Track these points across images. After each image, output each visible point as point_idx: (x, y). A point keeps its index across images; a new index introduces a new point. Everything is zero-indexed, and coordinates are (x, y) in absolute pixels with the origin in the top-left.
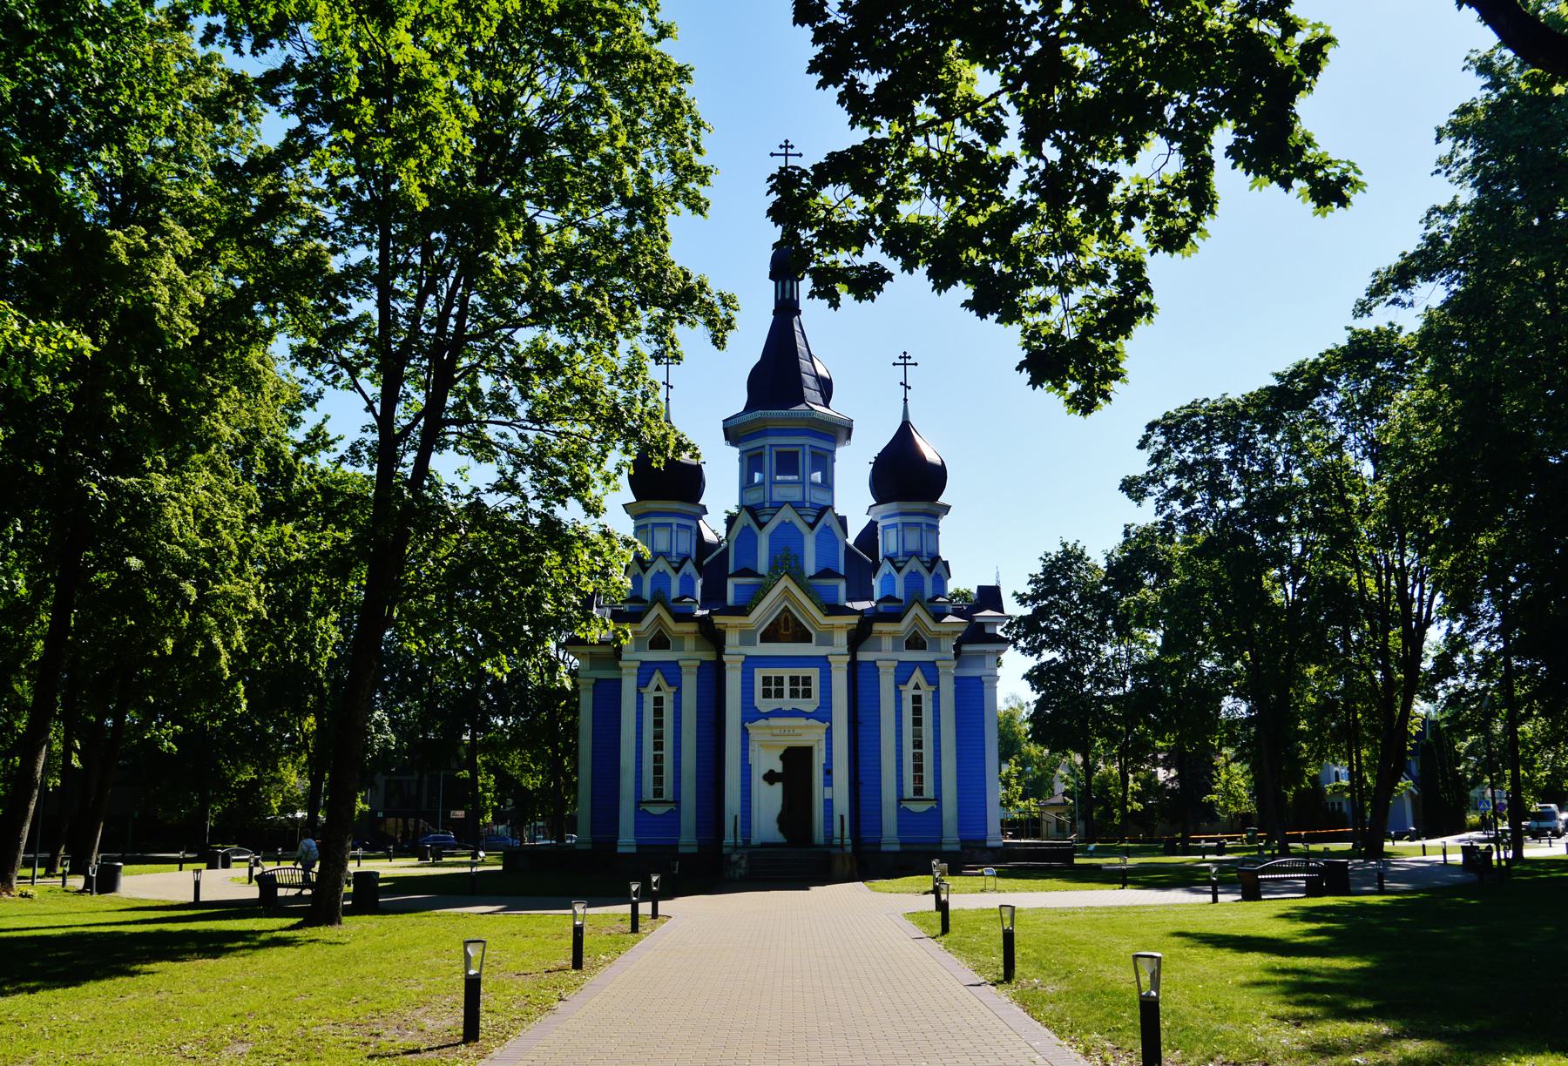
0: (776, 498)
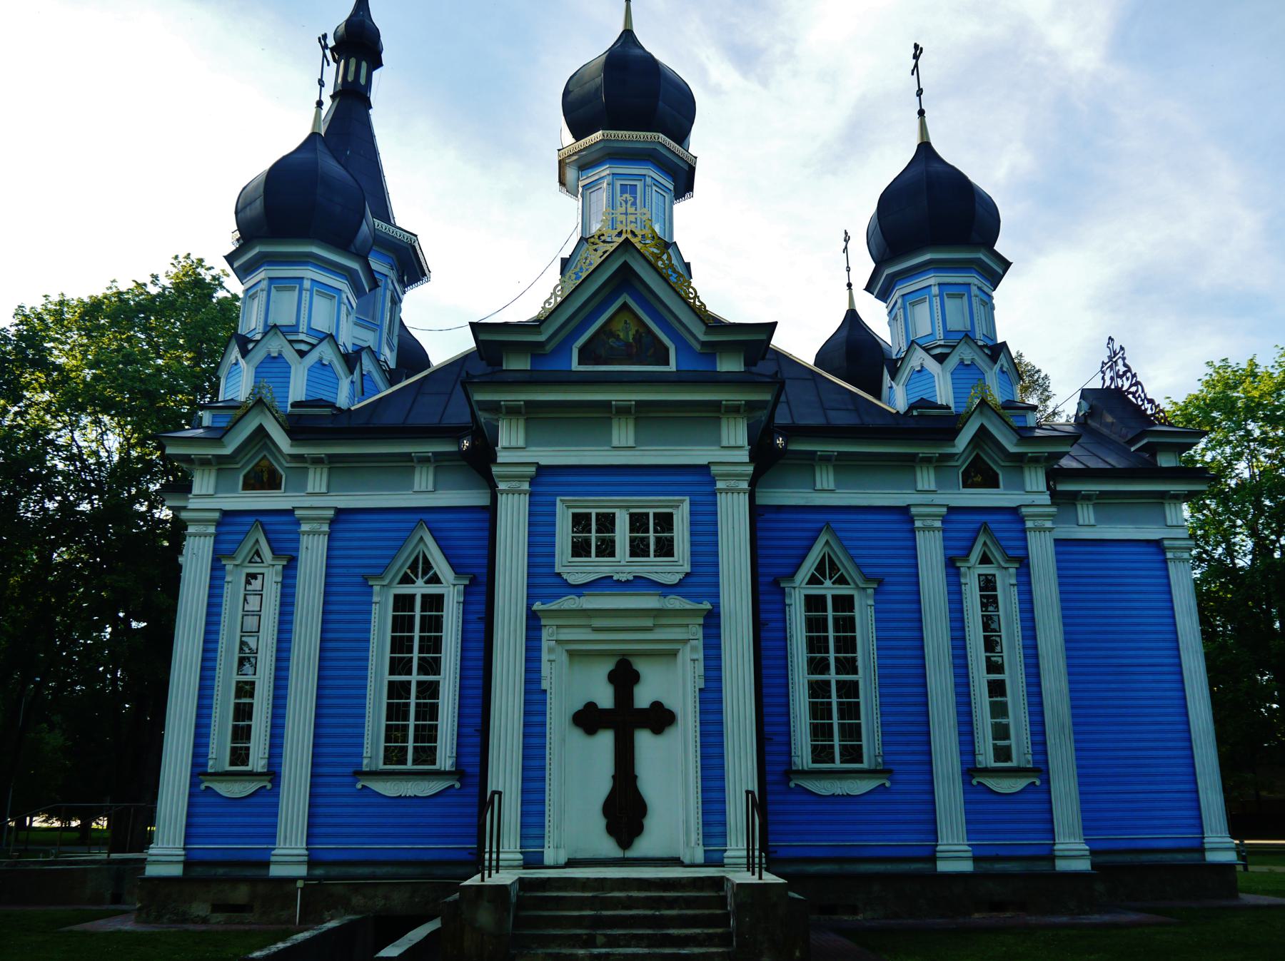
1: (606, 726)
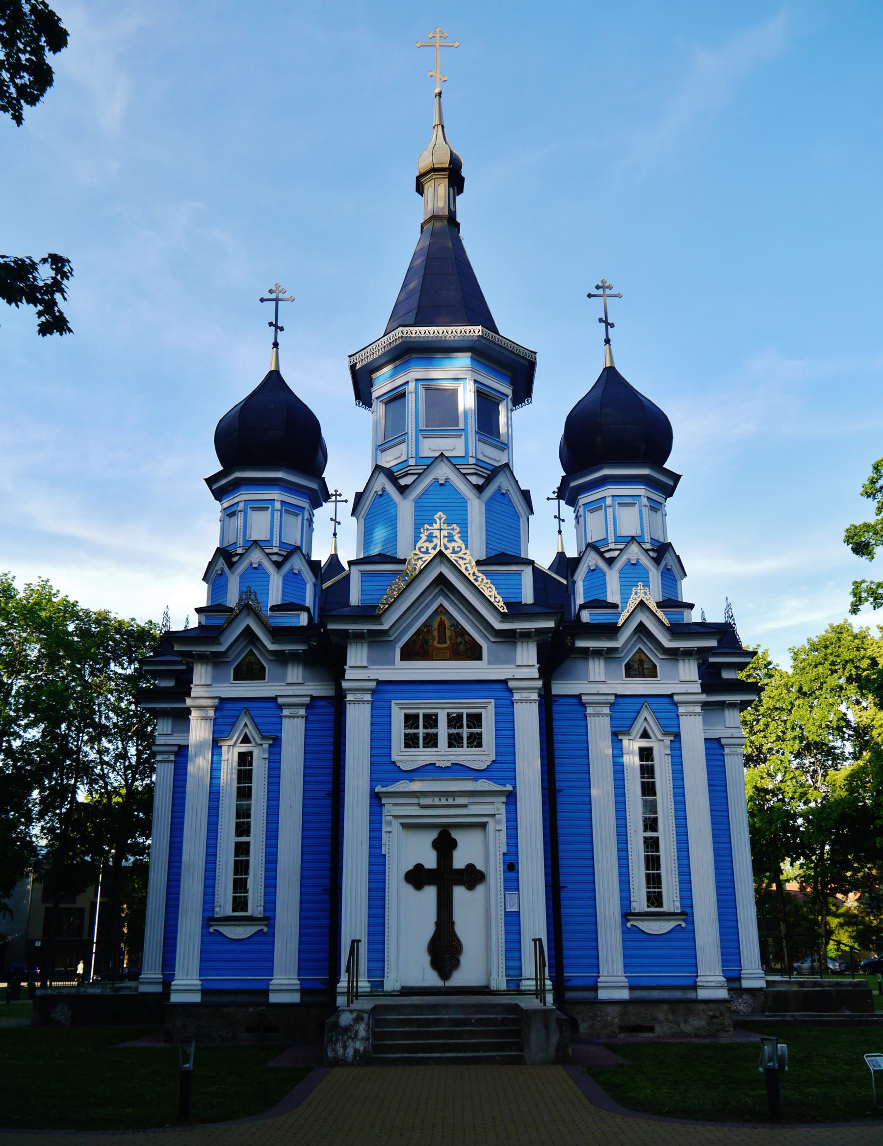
1: (430, 883)
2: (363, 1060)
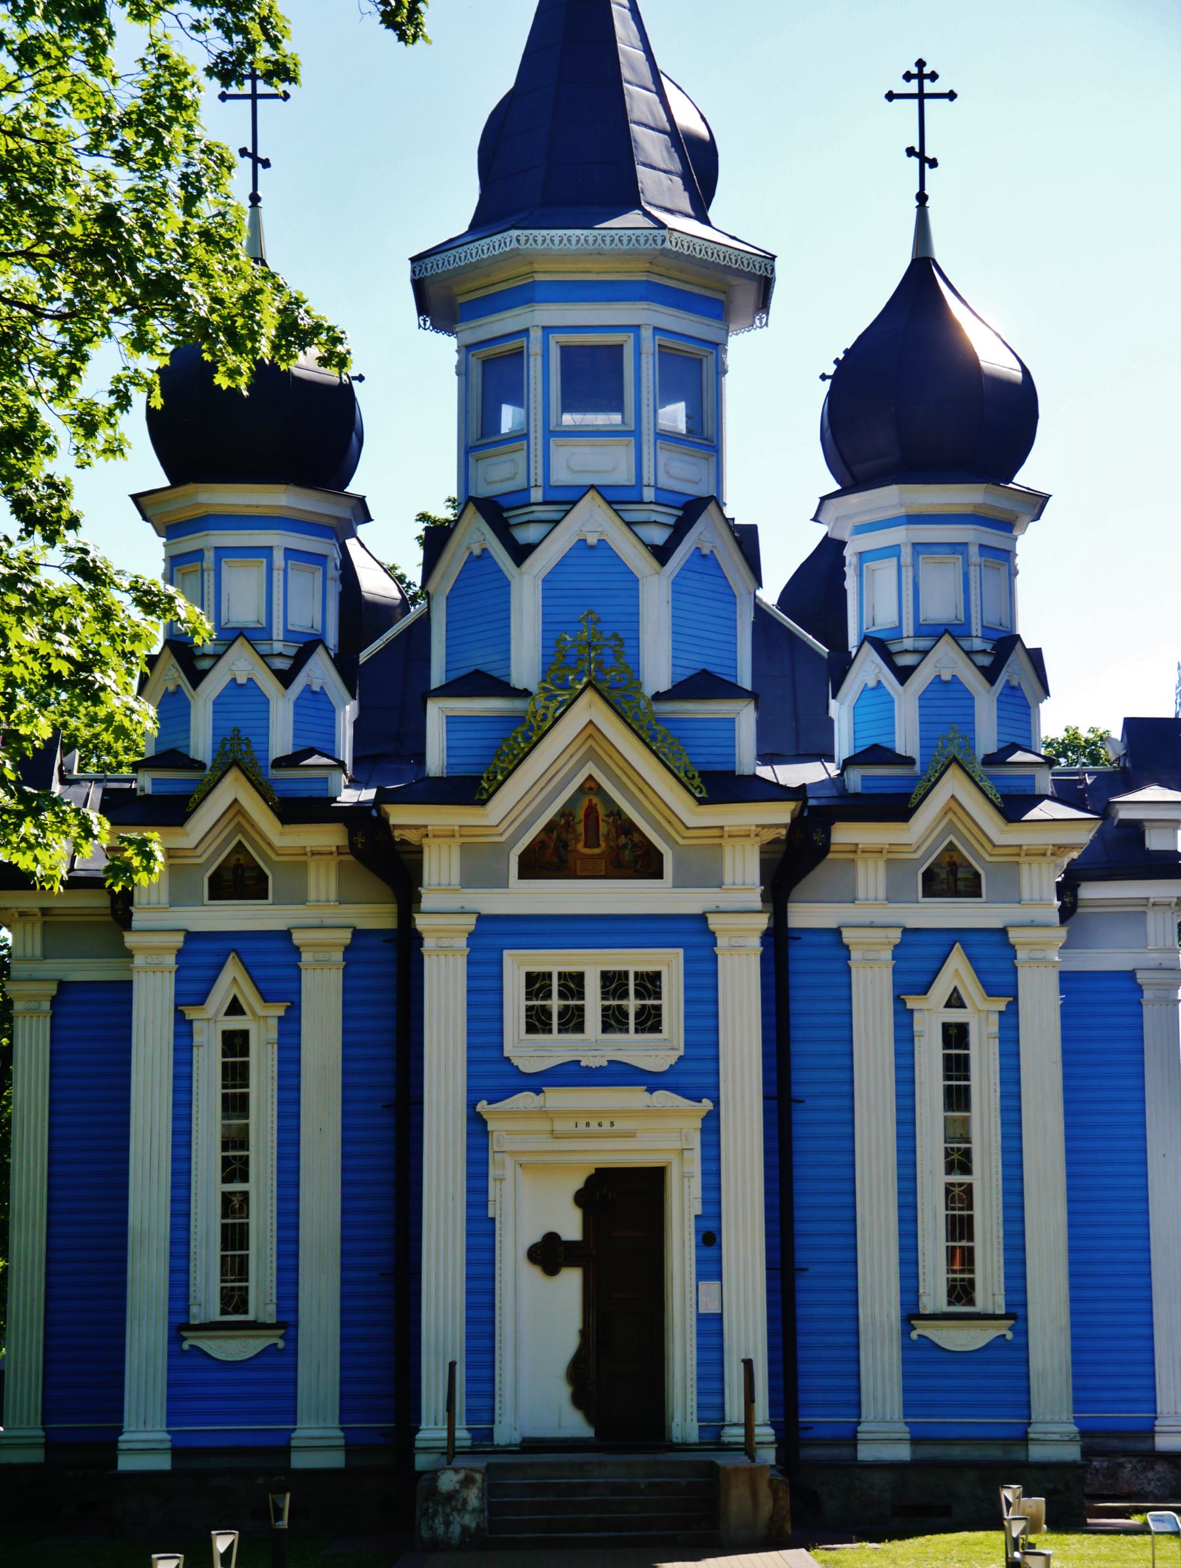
0: (561, 476)
2: (473, 1541)
